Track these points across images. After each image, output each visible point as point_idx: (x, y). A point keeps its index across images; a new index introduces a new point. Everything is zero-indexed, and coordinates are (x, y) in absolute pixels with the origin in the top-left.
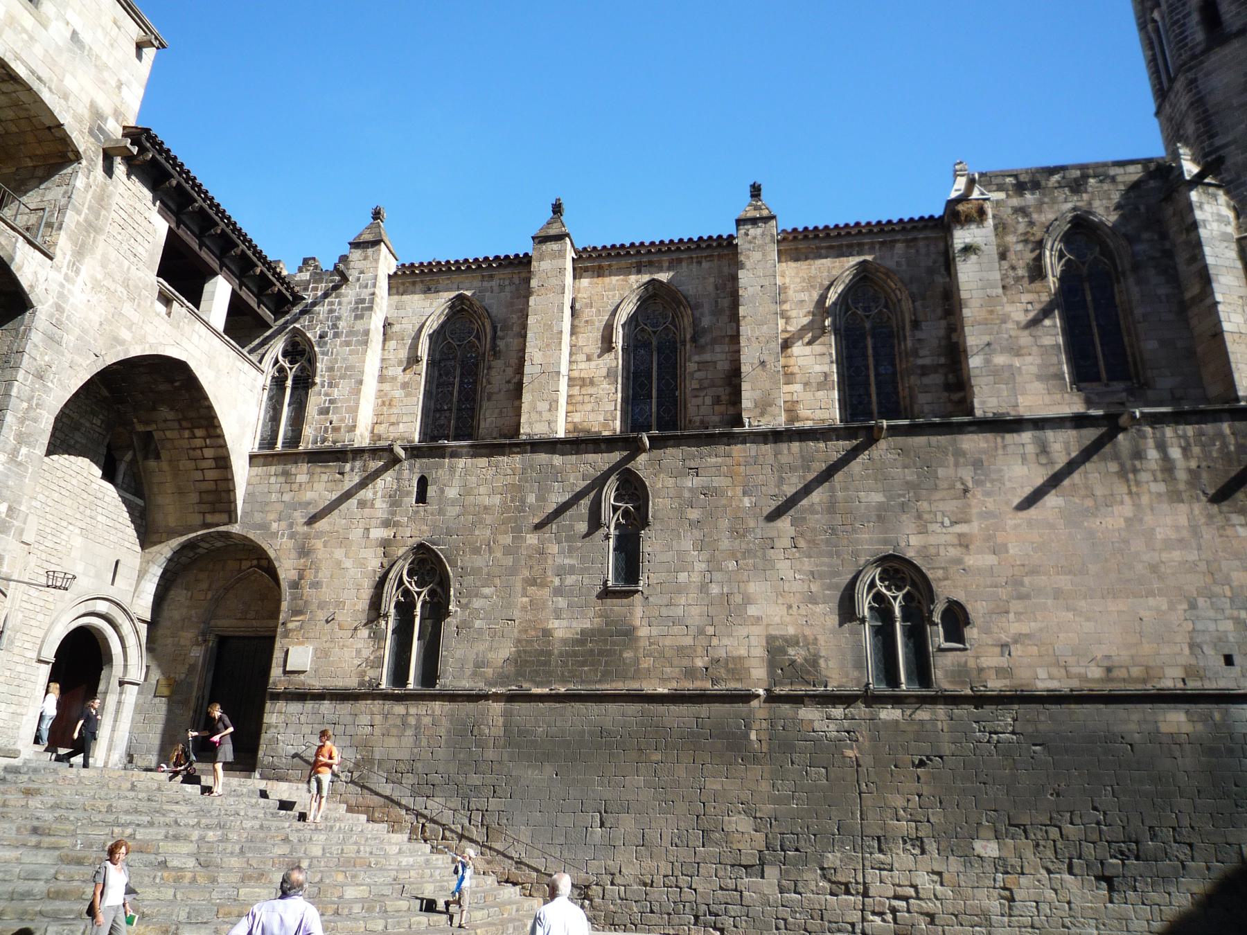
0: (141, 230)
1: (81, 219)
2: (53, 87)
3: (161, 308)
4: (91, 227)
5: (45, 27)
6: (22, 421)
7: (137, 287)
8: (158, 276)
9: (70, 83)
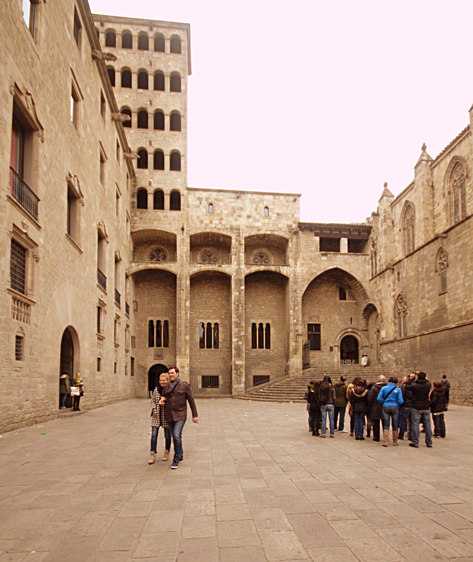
0: (311, 244)
1: (294, 253)
2: (277, 230)
3: (324, 258)
4: (297, 253)
5: (270, 219)
6: (294, 302)
7: (314, 258)
8: (320, 250)
9: (280, 225)
